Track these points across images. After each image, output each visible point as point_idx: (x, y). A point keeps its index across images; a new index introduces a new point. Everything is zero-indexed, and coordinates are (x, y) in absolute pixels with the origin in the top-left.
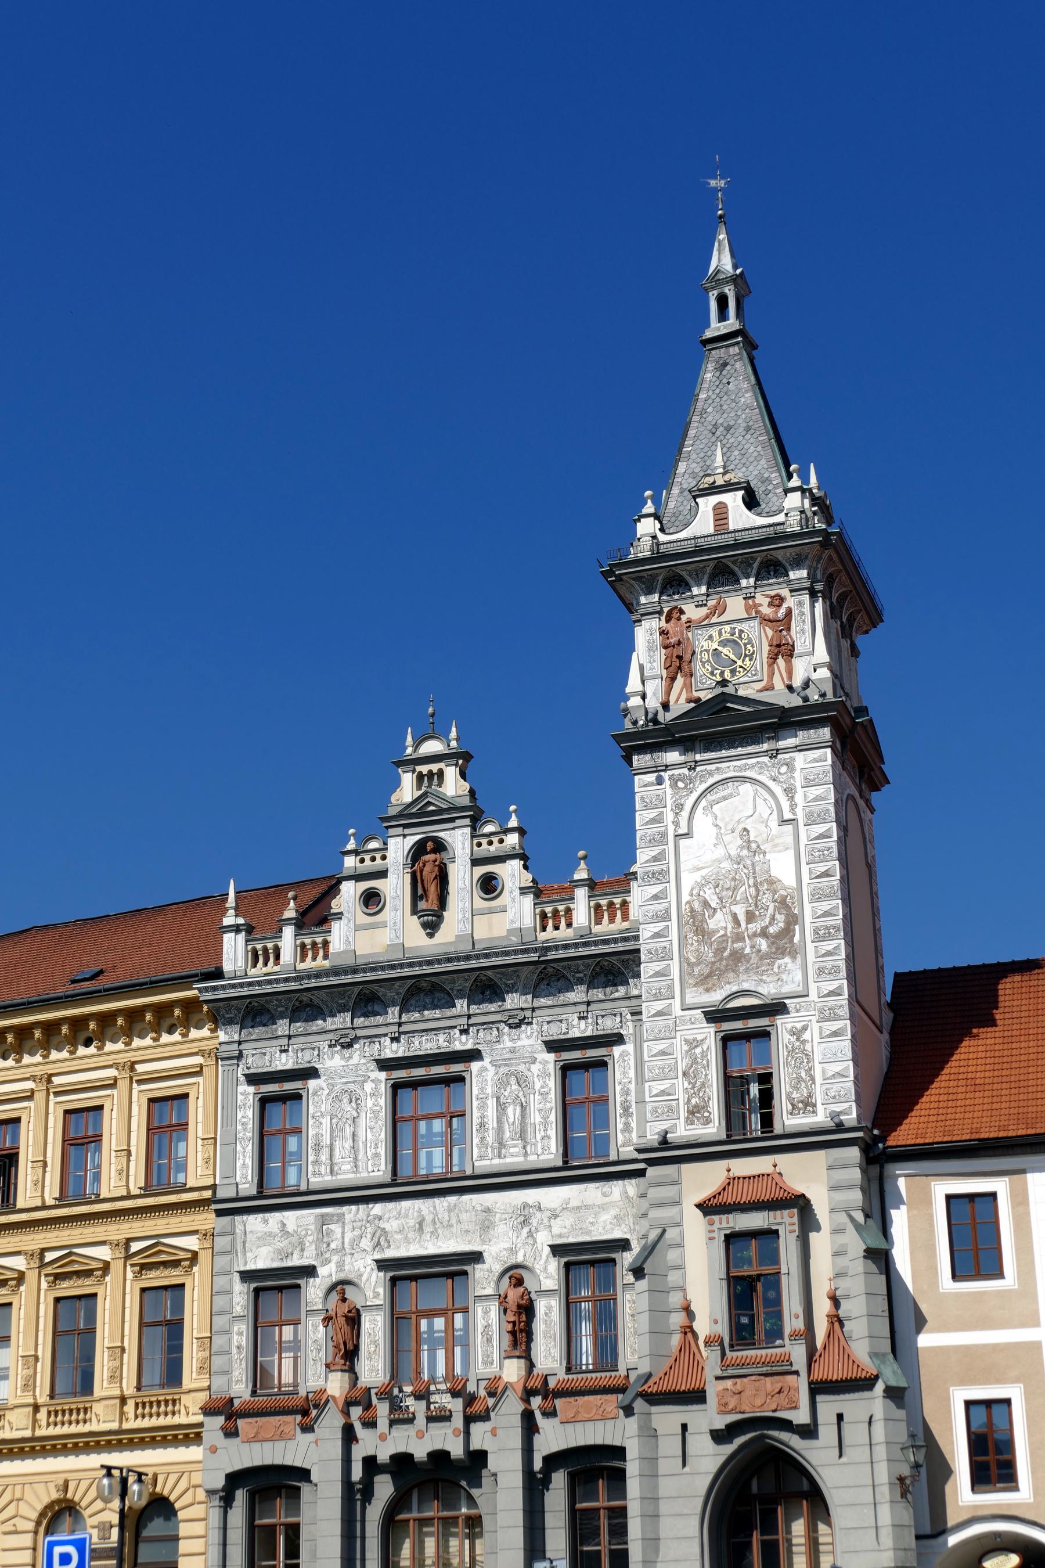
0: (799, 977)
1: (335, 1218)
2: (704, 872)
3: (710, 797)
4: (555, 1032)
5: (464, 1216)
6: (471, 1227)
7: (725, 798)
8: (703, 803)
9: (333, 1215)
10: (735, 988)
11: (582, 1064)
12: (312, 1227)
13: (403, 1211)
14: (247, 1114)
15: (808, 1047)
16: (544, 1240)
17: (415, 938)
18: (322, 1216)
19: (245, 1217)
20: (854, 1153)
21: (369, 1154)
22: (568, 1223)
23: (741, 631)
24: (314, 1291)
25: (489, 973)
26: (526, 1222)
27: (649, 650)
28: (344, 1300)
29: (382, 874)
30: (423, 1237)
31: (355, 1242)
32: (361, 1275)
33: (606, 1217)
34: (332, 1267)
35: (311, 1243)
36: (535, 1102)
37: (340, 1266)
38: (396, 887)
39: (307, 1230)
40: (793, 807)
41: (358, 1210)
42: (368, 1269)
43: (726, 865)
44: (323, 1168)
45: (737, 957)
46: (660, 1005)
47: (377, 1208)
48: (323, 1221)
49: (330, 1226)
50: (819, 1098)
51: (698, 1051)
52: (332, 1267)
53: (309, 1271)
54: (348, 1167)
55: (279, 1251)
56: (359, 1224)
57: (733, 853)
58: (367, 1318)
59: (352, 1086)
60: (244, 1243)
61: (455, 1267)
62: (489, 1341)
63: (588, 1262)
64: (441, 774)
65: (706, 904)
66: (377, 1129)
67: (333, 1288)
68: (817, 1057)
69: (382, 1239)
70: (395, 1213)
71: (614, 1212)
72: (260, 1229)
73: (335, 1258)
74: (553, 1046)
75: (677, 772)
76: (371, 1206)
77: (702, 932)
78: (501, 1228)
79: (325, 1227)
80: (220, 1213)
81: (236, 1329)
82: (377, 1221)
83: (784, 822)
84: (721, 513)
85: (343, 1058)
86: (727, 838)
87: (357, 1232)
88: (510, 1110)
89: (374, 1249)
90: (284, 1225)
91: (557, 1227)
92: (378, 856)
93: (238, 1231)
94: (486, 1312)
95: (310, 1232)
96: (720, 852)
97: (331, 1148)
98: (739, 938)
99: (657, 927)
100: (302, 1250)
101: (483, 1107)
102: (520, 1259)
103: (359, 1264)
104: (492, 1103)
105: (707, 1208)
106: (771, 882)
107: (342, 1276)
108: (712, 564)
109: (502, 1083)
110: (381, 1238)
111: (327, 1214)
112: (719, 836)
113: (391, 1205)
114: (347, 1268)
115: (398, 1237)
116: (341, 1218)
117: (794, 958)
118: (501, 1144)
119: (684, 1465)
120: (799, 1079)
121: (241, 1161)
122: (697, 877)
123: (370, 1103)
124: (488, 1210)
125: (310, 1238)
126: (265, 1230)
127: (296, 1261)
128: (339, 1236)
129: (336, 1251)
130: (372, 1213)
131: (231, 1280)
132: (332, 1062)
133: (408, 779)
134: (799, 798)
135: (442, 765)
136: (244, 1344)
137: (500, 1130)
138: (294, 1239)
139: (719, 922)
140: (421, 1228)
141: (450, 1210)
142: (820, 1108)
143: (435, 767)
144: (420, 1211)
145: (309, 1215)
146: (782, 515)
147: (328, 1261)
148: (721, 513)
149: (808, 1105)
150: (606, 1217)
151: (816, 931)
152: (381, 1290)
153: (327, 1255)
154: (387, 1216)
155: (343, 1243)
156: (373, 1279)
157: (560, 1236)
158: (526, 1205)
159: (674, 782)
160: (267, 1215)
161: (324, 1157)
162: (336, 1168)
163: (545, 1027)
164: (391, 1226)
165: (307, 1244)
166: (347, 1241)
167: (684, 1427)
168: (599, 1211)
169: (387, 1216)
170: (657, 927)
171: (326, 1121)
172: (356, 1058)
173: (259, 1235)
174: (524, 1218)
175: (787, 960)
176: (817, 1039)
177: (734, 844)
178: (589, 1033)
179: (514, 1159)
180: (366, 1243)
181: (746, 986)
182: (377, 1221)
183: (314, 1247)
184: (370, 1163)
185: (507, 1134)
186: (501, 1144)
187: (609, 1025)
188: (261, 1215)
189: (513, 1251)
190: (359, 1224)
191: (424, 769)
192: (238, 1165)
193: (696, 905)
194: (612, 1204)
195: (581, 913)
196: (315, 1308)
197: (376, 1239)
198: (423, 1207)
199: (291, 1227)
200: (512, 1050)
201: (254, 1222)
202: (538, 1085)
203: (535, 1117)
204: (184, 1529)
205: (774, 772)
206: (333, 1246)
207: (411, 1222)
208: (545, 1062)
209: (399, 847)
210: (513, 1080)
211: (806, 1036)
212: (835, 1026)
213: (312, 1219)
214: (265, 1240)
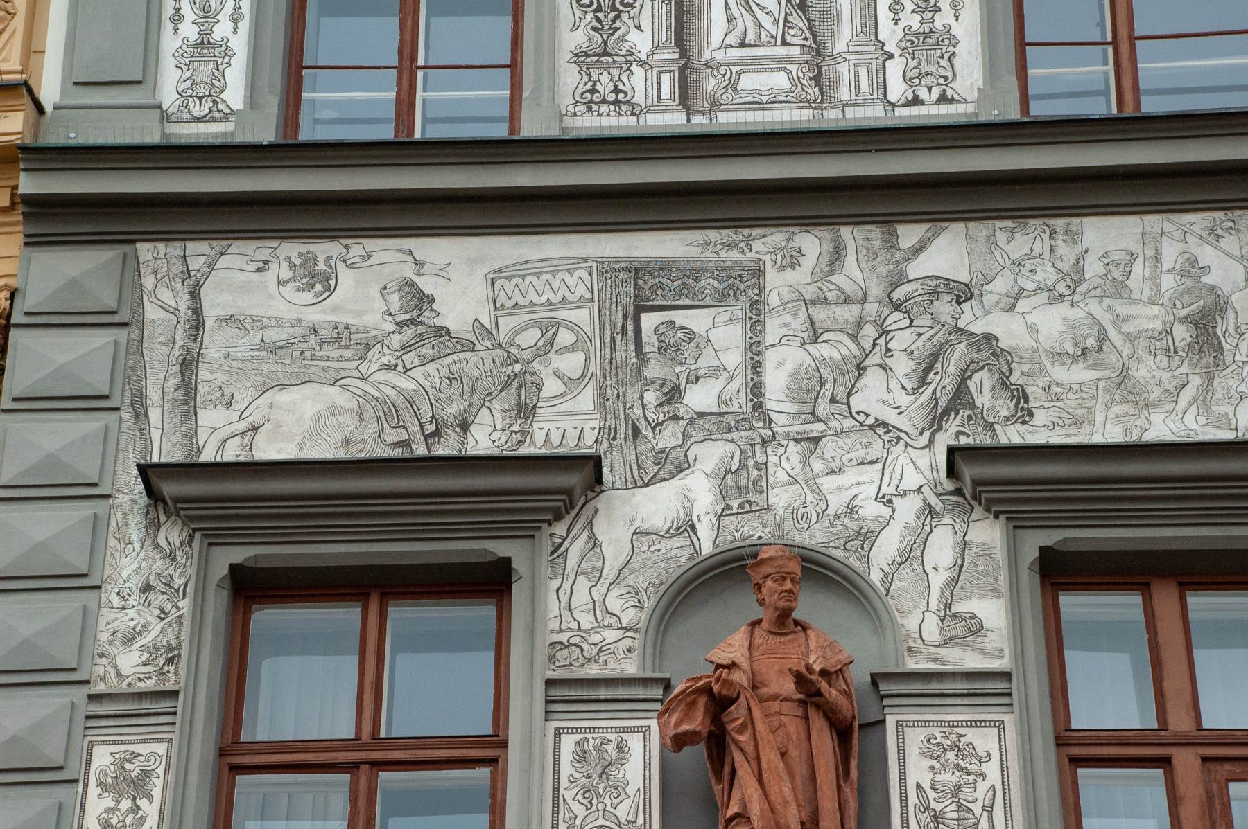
1: (709, 283)
9: (697, 272)
12: (582, 316)
13: (1093, 268)
18: (637, 271)
19: (198, 252)
21: (889, 33)
24: (593, 594)
28: (785, 622)
30: (1225, 381)
32: (866, 537)
34: (697, 491)
35: (571, 384)
37: (742, 488)
39: (550, 328)
41: (838, 254)
42: (908, 509)
44: (638, 80)
47: (946, 252)
48: (642, 290)
49: (679, 317)
52: (697, 491)
53: (572, 482)
54: (780, 81)
55: (390, 413)
56: (848, 314)
58: (915, 739)
60: (188, 366)
67: (729, 571)
69: (983, 386)
70: (1047, 274)
72: (280, 308)
73: (711, 455)
76: (909, 234)
79: (649, 321)
80: (51, 220)
81: (103, 758)
82: (945, 308)
87: (835, 349)
89: (936, 422)
90: (423, 300)
93: (152, 312)
95: (565, 337)
100: (525, 411)
107: (755, 530)
111: (664, 267)
113: (1020, 241)
114: (780, 498)
115: (1080, 374)
116: (741, 288)
121: (189, 30)
125: (572, 363)
126: (314, 315)
128: (733, 359)
129: (717, 423)
130: (916, 269)
131: (96, 525)
138: (472, 363)
144: (1191, 269)
145: (564, 269)
147: (671, 465)
152: (991, 612)
153: (669, 438)
154: (1001, 285)
155: (757, 390)
156: (941, 549)
160: (325, 250)
162: (710, 84)
164: (1033, 327)
165: (552, 386)
166: (776, 382)
169: (1001, 285)
173: (274, 335)
182: (945, 308)
183: (587, 399)
184: (894, 70)
188: (293, 250)
190: (848, 314)
192: (170, 43)
196: (593, 671)
197: (944, 381)
198: (1207, 255)
201: (252, 284)
206: (699, 398)
207: (1149, 318)
213: (578, 283)
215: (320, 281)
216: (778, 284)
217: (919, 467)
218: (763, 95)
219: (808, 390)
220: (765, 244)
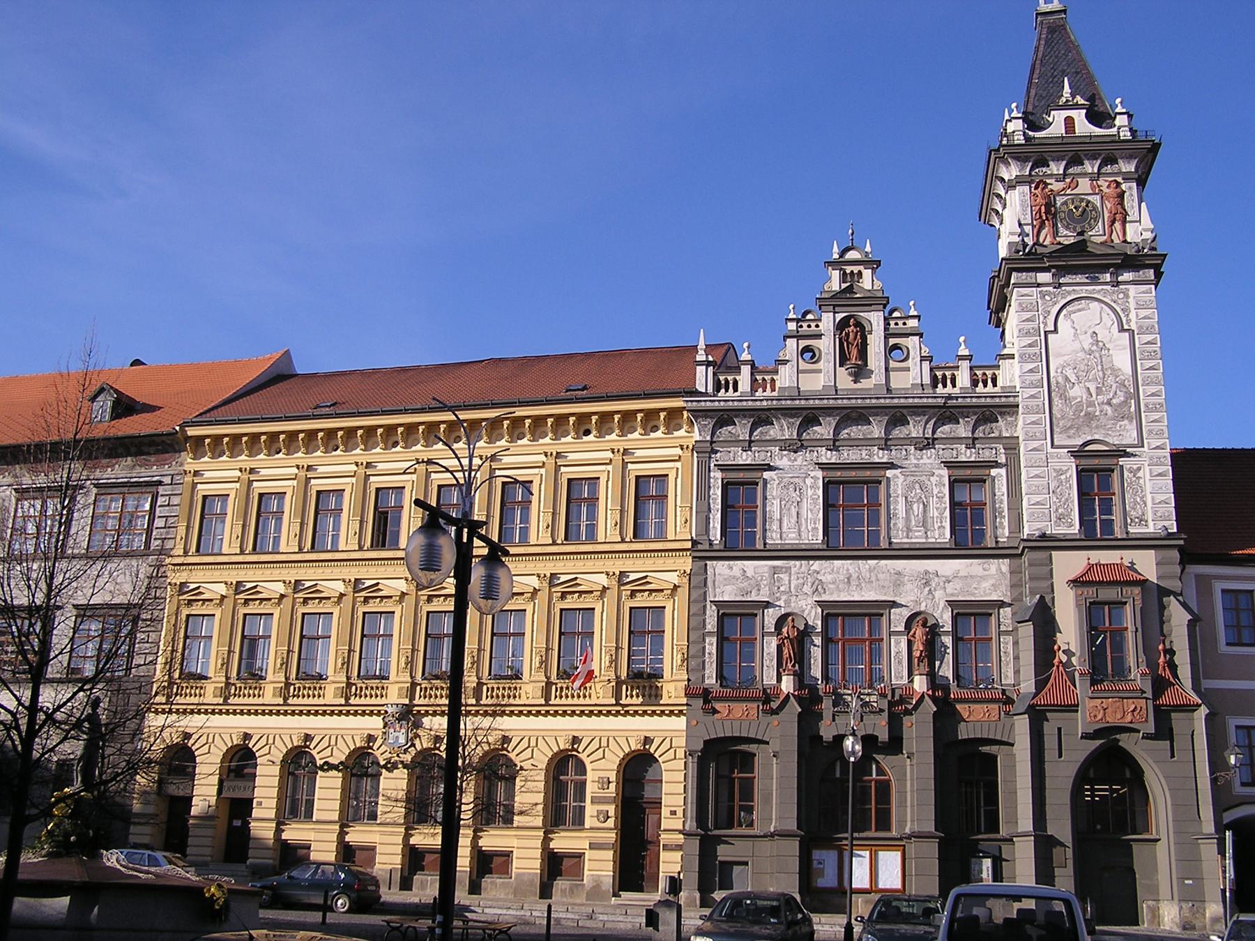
0: (1135, 434)
2: (1066, 358)
3: (1069, 308)
4: (948, 456)
5: (881, 576)
6: (886, 584)
7: (1080, 310)
8: (1064, 312)
10: (1089, 438)
11: (966, 480)
14: (716, 493)
15: (1141, 481)
16: (940, 597)
17: (845, 381)
20: (1176, 554)
22: (958, 587)
23: (1089, 202)
25: (904, 411)
26: (927, 583)
27: (1022, 205)
29: (819, 336)
31: (800, 587)
33: (986, 585)
36: (933, 502)
37: (788, 602)
38: (827, 345)
40: (1129, 321)
43: (1082, 355)
45: (1090, 417)
46: (1035, 444)
47: (816, 565)
48: (775, 570)
50: (1150, 516)
51: (1063, 477)
53: (767, 605)
55: (741, 589)
57: (1086, 347)
59: (797, 480)
61: (875, 611)
62: (900, 662)
63: (971, 614)
64: (860, 273)
65: (1067, 379)
66: (815, 510)
68: (1148, 489)
71: (992, 581)
73: (784, 598)
74: (949, 465)
75: (1045, 289)
77: (1064, 396)
78: (909, 586)
83: (1122, 330)
84: (1069, 122)
85: (790, 460)
86: (1082, 337)
87: (801, 581)
88: (915, 506)
91: (950, 588)
92: (813, 325)
94: (898, 643)
96: (1077, 346)
97: (781, 521)
98: (1091, 404)
99: (1033, 391)
101: (896, 502)
102: (923, 609)
103: (802, 603)
104: (902, 501)
105: (1076, 582)
106: (1113, 369)
108: (1071, 154)
109: (910, 488)
110: (819, 586)
112: (1076, 335)
117: (1131, 421)
118: (909, 529)
119: (1060, 756)
120: (1135, 502)
122: (1061, 361)
123: (810, 492)
124: (899, 573)
127: (753, 597)
132: (782, 460)
133: (836, 274)
134: (1132, 316)
135: (861, 268)
136: (714, 651)
137: (908, 519)
139: (1077, 392)
140: (849, 581)
141: (870, 570)
142: (1151, 524)
143: (856, 269)
146: (1115, 129)
148: (1069, 122)
149: (1142, 520)
150: (986, 585)
151: (1146, 406)
157: (952, 595)
158: (927, 572)
159: (1043, 296)
161: (775, 527)
163: (941, 452)
167: (1059, 729)
168: (985, 579)
170: (1033, 391)
171: (776, 502)
172: (799, 461)
174: (926, 580)
175: (1126, 422)
176: (1148, 477)
177: (1087, 342)
178: (972, 459)
179: (918, 538)
180: (807, 589)
181: (1097, 437)
185: (913, 523)
186: (909, 529)
187: (987, 455)
189: (918, 602)
191: (848, 269)
193: (1060, 380)
194: (991, 576)
195: (963, 379)
199: (749, 574)
200: (917, 466)
202: (935, 492)
203: (933, 513)
204: (665, 777)
205: (1115, 297)
206: (782, 589)
207: (842, 577)
208: (941, 476)
209: (828, 322)
210: (917, 486)
211: (1140, 474)
212: (1161, 469)
213: (766, 569)
214: (731, 580)
215: (731, 568)
216: (793, 570)
217: (811, 600)
218: (791, 539)
219: (797, 587)
220: (792, 563)
